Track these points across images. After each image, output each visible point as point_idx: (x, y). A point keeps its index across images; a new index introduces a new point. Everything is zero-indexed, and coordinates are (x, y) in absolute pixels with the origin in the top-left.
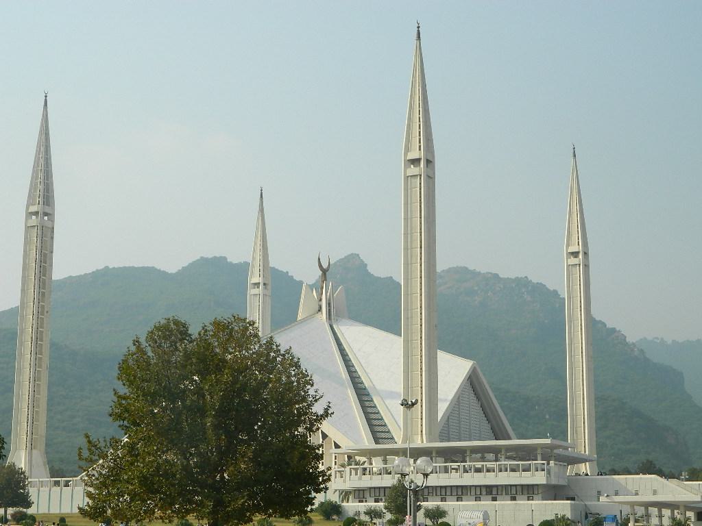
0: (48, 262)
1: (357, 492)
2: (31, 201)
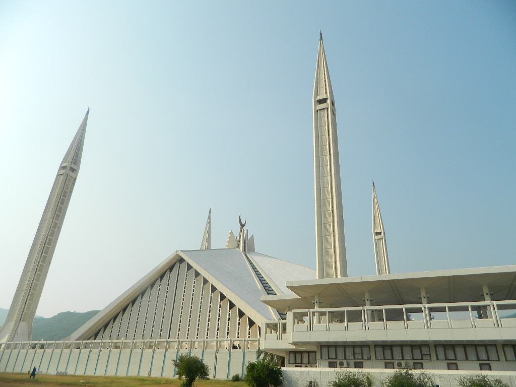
0: (67, 196)
1: (292, 356)
2: (65, 160)
